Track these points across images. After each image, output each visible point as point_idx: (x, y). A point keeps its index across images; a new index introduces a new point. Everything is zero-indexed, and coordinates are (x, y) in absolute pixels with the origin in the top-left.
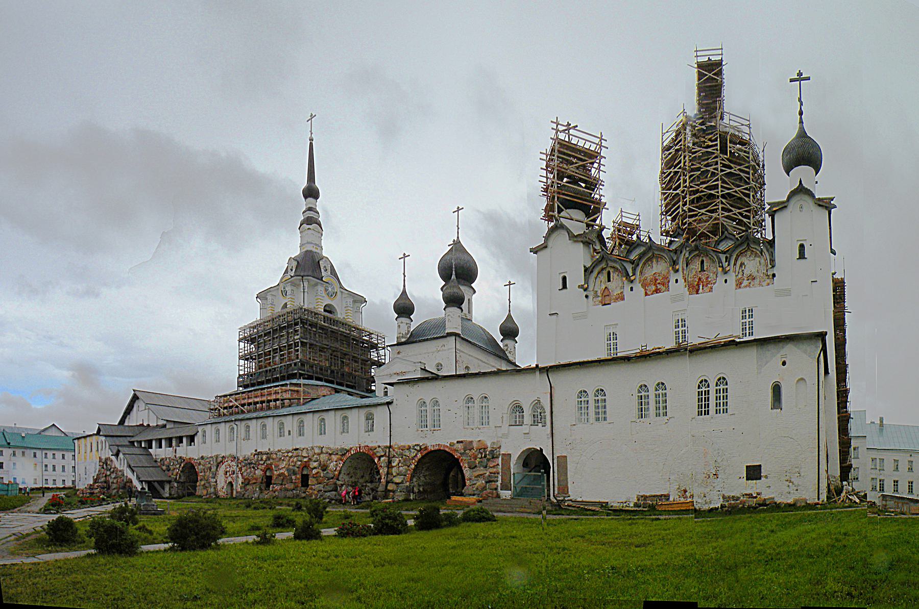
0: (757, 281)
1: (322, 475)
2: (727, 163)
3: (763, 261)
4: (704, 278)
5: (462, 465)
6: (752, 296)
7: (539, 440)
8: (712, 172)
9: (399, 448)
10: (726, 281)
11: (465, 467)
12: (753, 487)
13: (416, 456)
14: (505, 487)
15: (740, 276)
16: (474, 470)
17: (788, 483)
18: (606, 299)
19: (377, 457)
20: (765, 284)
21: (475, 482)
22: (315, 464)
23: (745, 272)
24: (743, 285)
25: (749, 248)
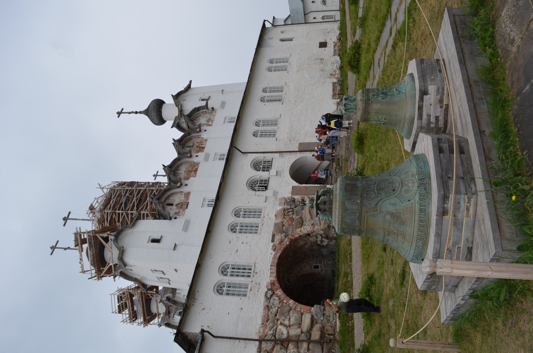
0: (212, 117)
4: (197, 145)
5: (297, 236)
8: (131, 213)
11: (301, 231)
13: (279, 297)
16: (304, 220)
20: (214, 114)
23: (204, 123)
25: (192, 121)
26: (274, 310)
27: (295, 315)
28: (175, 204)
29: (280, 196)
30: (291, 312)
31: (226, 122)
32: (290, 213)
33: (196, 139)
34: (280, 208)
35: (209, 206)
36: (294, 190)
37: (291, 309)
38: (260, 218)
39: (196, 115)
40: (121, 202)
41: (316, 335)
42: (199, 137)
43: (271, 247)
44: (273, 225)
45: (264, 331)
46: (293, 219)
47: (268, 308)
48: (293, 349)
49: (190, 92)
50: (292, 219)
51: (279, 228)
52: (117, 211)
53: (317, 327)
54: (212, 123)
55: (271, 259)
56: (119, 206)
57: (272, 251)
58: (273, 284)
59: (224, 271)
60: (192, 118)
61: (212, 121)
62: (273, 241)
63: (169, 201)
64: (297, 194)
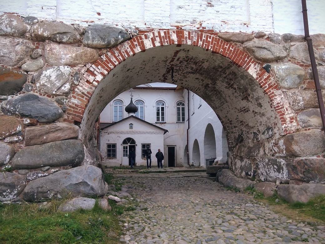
48: (304, 100)
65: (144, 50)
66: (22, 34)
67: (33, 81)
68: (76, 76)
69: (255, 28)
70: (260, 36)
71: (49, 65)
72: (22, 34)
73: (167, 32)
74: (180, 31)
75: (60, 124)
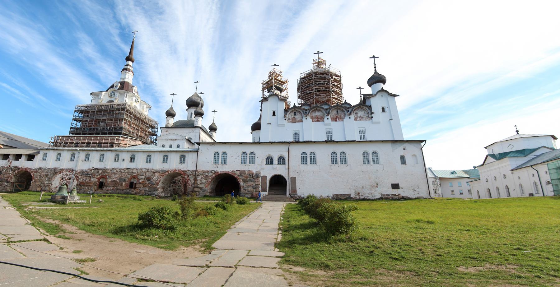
0: (364, 119)
1: (147, 183)
2: (333, 81)
3: (366, 112)
5: (239, 180)
6: (365, 124)
7: (281, 170)
9: (201, 172)
10: (350, 118)
12: (395, 192)
14: (264, 190)
15: (356, 117)
16: (246, 183)
17: (413, 191)
18: (294, 121)
19: (187, 175)
20: (367, 120)
21: (247, 188)
22: (143, 177)
23: (358, 115)
24: (358, 120)
26: (207, 174)
27: (204, 182)
28: (295, 116)
29: (261, 172)
30: (206, 180)
31: (360, 129)
32: (250, 177)
33: (344, 114)
34: (254, 172)
35: (294, 134)
36: (264, 178)
37: (207, 180)
38: (249, 164)
39: (366, 109)
40: (320, 81)
41: (196, 189)
42: (345, 116)
43: (233, 170)
44: (245, 170)
45: (200, 172)
46: (247, 178)
47: (208, 172)
49: (390, 98)
50: (247, 177)
51: (242, 172)
52: (314, 82)
53: (199, 190)
54: (359, 120)
55: (228, 171)
56: (318, 81)
57: (232, 171)
58: (218, 173)
59: (225, 153)
60: (362, 106)
61: (360, 120)
62: (236, 170)
63: (296, 113)
64: (262, 178)
65: (169, 173)
66: (152, 172)
67: (152, 179)
68: (158, 178)
69: (188, 169)
70: (188, 170)
71: (155, 176)
72: (152, 172)
73: (173, 170)
74: (175, 170)
75: (155, 185)
